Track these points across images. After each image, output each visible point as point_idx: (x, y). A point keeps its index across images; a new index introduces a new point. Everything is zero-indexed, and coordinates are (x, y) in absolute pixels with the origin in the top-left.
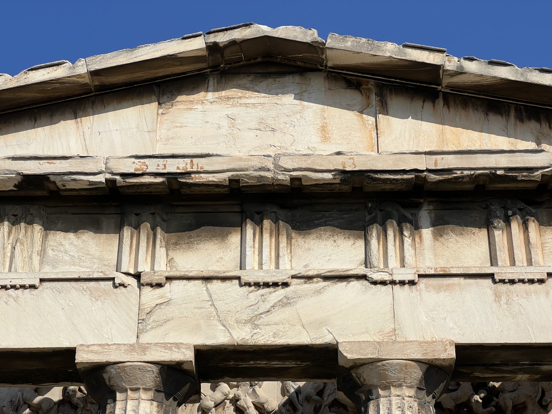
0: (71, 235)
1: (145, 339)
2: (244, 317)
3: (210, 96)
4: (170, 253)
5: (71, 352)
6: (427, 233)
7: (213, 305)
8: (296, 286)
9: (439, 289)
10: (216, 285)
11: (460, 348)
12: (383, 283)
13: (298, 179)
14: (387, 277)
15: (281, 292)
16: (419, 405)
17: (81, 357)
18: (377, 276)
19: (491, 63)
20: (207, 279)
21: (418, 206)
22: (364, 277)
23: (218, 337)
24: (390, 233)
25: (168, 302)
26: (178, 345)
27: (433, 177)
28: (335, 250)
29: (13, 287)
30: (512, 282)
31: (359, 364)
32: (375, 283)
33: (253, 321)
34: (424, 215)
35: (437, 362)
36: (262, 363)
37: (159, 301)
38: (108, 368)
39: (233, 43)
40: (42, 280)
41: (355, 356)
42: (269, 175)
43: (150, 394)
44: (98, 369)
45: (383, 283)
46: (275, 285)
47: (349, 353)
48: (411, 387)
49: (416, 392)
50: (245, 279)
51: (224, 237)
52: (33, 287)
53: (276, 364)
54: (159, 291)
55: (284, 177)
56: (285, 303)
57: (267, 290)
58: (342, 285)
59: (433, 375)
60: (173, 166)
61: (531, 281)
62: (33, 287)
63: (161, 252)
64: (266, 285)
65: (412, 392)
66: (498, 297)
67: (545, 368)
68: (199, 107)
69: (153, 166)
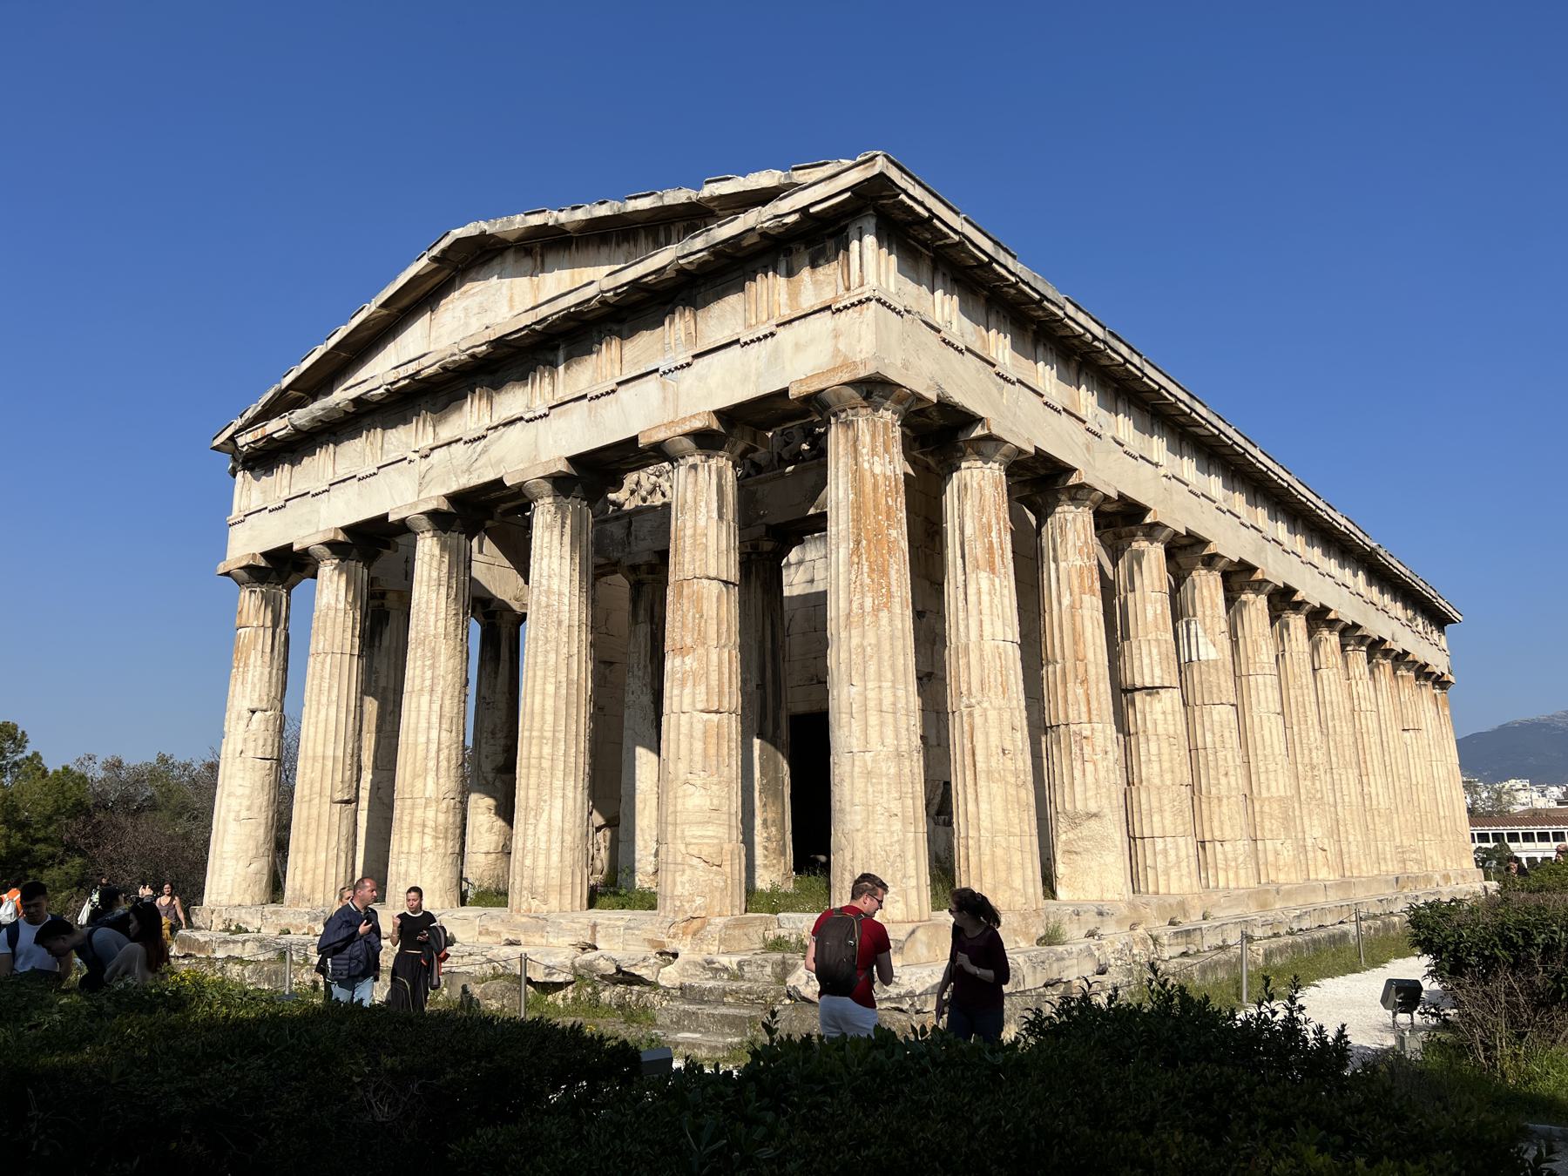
1: (422, 496)
3: (456, 294)
6: (561, 368)
8: (492, 435)
9: (560, 416)
11: (572, 460)
13: (473, 356)
15: (483, 442)
18: (527, 417)
19: (574, 209)
20: (449, 444)
21: (557, 348)
22: (521, 419)
23: (454, 486)
28: (513, 401)
33: (468, 470)
34: (561, 354)
39: (443, 251)
51: (460, 408)
56: (484, 451)
59: (560, 484)
63: (430, 429)
65: (551, 500)
69: (403, 372)
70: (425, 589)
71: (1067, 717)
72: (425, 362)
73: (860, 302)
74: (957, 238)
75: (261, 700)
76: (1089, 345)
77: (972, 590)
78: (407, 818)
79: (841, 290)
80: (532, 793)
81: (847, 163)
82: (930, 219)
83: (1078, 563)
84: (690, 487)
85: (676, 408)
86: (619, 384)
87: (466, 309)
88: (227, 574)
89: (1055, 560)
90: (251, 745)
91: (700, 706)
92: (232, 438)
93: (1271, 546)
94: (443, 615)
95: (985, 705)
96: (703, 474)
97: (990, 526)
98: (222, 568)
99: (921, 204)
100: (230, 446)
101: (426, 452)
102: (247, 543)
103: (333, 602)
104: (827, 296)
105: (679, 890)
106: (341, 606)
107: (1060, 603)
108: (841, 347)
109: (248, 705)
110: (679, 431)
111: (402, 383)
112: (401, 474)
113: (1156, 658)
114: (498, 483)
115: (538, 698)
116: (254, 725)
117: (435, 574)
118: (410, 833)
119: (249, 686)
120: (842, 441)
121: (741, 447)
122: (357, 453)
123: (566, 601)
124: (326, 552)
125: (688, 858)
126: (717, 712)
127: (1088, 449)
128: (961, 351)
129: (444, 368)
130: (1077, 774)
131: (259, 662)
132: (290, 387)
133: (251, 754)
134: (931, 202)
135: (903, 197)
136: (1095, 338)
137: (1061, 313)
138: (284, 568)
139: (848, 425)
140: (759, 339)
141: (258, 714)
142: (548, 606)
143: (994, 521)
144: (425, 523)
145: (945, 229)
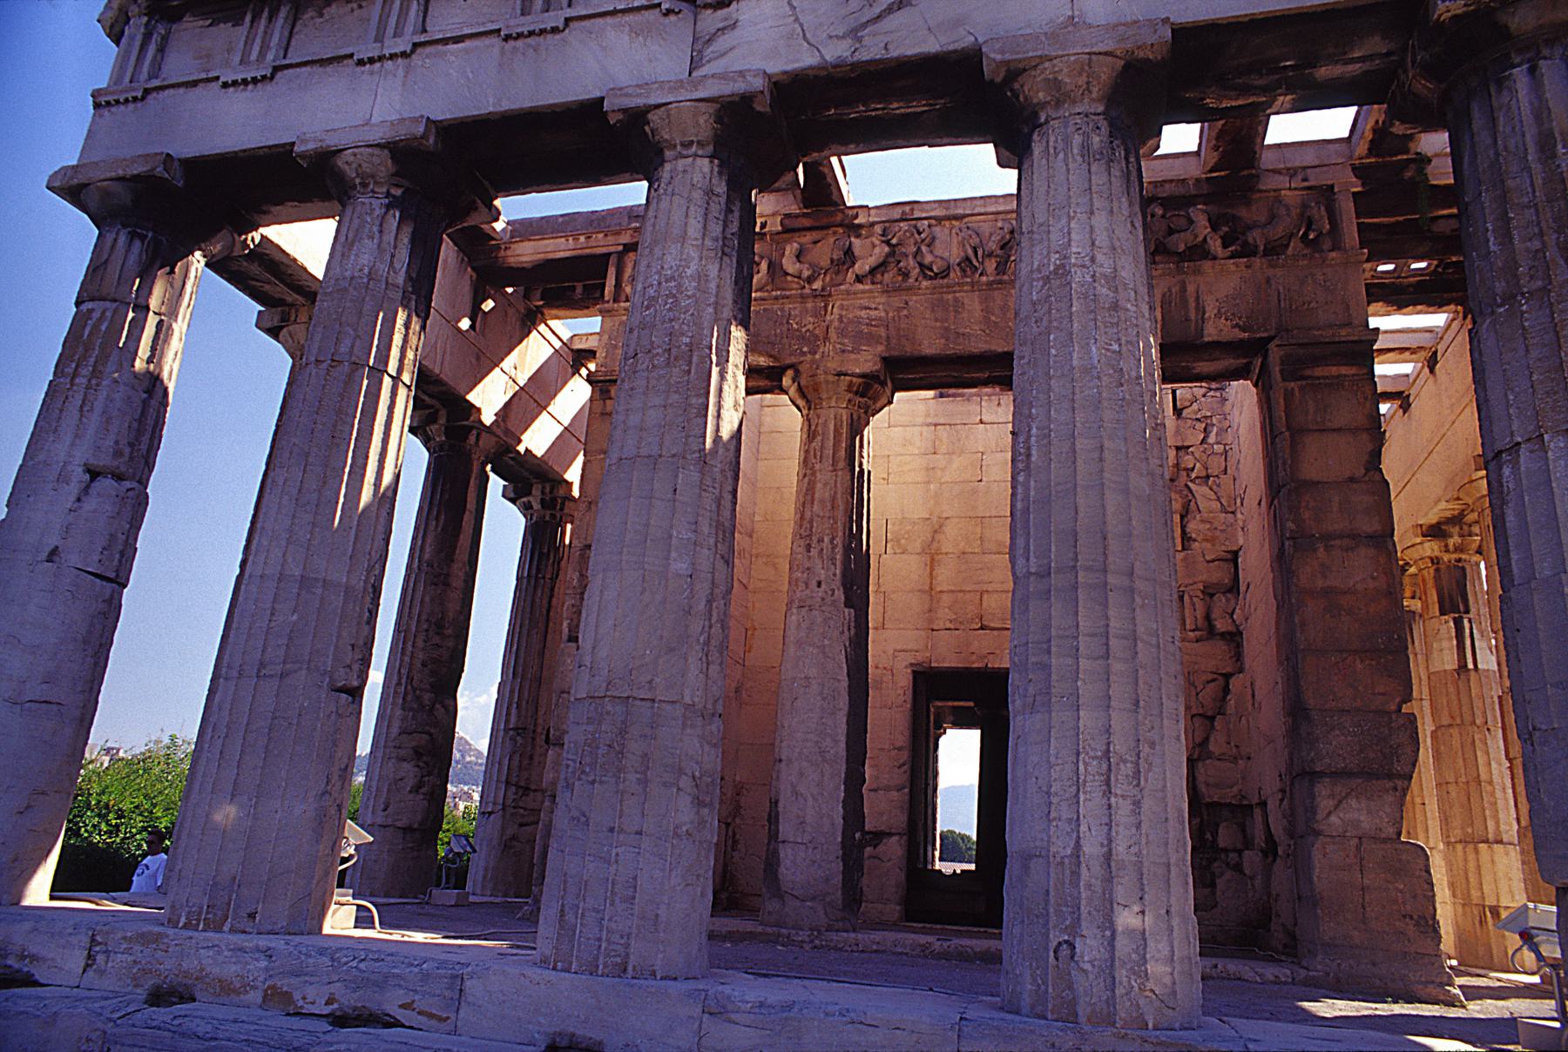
7: (797, 20)
16: (1111, 125)
25: (734, 26)
26: (741, 73)
29: (531, 33)
31: (1015, 72)
33: (855, 33)
35: (1141, 54)
36: (877, 109)
37: (721, 25)
38: (650, 116)
40: (568, 21)
41: (1007, 57)
43: (710, 148)
44: (637, 117)
48: (1099, 100)
49: (1107, 108)
52: (555, 30)
53: (897, 108)
62: (555, 30)
67: (1324, 72)
75: (118, 454)
78: (635, 747)
80: (1120, 721)
103: (383, 268)
106: (400, 280)
112: (635, 32)
115: (1112, 500)
116: (90, 504)
117: (716, 229)
118: (644, 782)
119: (94, 420)
123: (1145, 309)
124: (383, 164)
142: (1115, 307)
144: (704, 125)
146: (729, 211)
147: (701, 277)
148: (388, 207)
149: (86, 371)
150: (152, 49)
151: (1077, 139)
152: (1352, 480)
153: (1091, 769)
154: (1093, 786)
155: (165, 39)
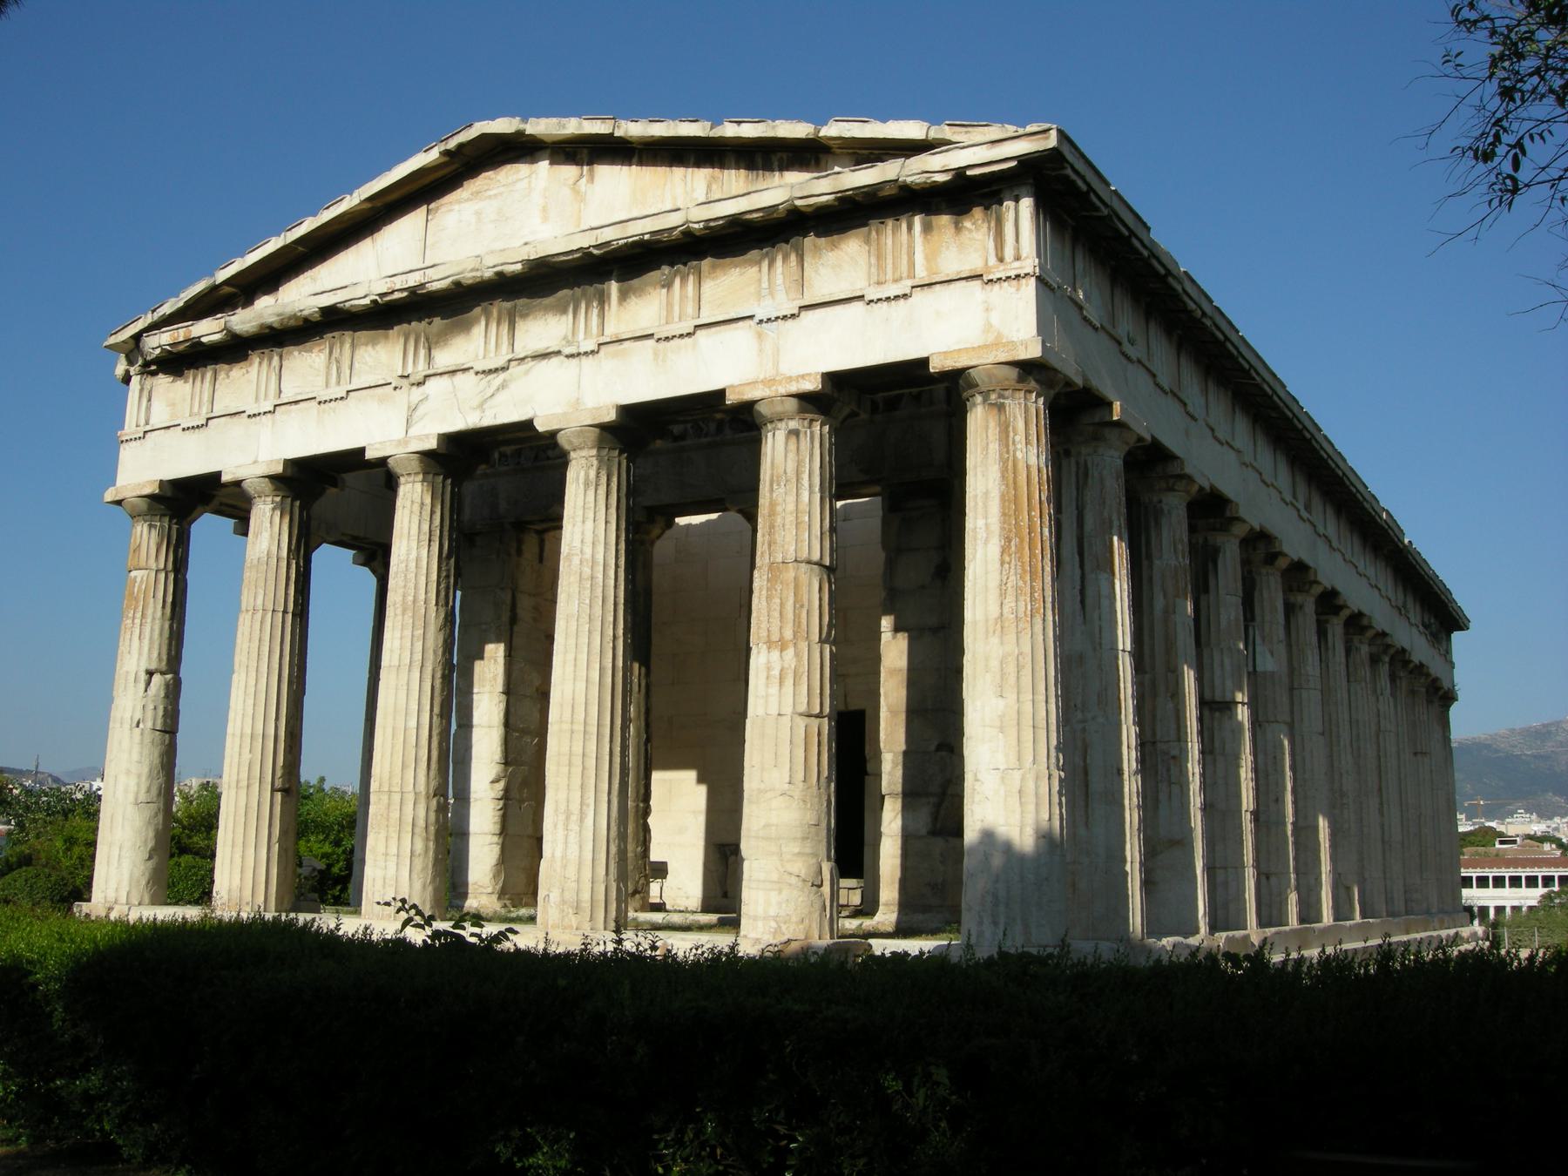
0: (370, 348)
2: (476, 403)
4: (434, 352)
5: (362, 450)
8: (515, 369)
10: (460, 376)
12: (572, 356)
14: (573, 350)
15: (502, 376)
17: (369, 455)
18: (567, 351)
20: (454, 372)
22: (559, 353)
24: (583, 305)
26: (427, 436)
27: (595, 252)
30: (667, 339)
31: (553, 435)
32: (567, 356)
33: (481, 406)
39: (461, 146)
42: (478, 274)
43: (420, 477)
45: (572, 356)
46: (496, 370)
47: (541, 427)
50: (479, 367)
54: (422, 388)
55: (488, 274)
56: (503, 386)
57: (491, 377)
58: (544, 364)
60: (412, 280)
61: (681, 336)
63: (422, 352)
64: (490, 372)
65: (594, 452)
66: (656, 354)
68: (456, 207)
69: (399, 283)
70: (414, 544)
71: (1154, 734)
72: (432, 274)
73: (1018, 276)
74: (1105, 212)
76: (1199, 321)
77: (1090, 592)
79: (992, 261)
81: (1011, 130)
82: (1088, 193)
83: (1173, 563)
84: (792, 455)
85: (776, 363)
86: (697, 327)
87: (478, 213)
88: (119, 503)
89: (1149, 557)
90: (150, 714)
91: (803, 708)
92: (137, 338)
93: (1320, 543)
94: (434, 576)
95: (1101, 720)
96: (805, 443)
97: (1111, 522)
98: (109, 495)
99: (1083, 178)
100: (132, 342)
101: (419, 377)
102: (143, 467)
104: (973, 263)
105: (772, 913)
107: (1151, 606)
108: (995, 318)
109: (144, 666)
110: (782, 390)
111: (397, 296)
113: (1228, 667)
114: (528, 425)
117: (426, 527)
120: (992, 424)
121: (846, 411)
122: (306, 367)
124: (267, 486)
125: (786, 877)
126: (817, 716)
127: (1187, 433)
128: (1096, 329)
129: (457, 284)
130: (1163, 797)
131: (159, 613)
132: (227, 282)
133: (149, 724)
134: (1090, 177)
135: (1069, 171)
136: (1204, 314)
137: (1179, 288)
138: (189, 501)
139: (1001, 408)
140: (888, 299)
141: (157, 678)
143: (1114, 517)
144: (415, 465)
145: (1098, 203)
146: (432, 513)
147: (418, 560)
148: (274, 509)
149: (139, 615)
150: (145, 400)
151: (582, 474)
152: (923, 587)
153: (562, 817)
154: (560, 826)
155: (150, 392)
